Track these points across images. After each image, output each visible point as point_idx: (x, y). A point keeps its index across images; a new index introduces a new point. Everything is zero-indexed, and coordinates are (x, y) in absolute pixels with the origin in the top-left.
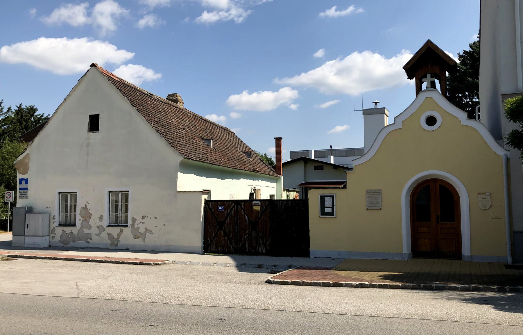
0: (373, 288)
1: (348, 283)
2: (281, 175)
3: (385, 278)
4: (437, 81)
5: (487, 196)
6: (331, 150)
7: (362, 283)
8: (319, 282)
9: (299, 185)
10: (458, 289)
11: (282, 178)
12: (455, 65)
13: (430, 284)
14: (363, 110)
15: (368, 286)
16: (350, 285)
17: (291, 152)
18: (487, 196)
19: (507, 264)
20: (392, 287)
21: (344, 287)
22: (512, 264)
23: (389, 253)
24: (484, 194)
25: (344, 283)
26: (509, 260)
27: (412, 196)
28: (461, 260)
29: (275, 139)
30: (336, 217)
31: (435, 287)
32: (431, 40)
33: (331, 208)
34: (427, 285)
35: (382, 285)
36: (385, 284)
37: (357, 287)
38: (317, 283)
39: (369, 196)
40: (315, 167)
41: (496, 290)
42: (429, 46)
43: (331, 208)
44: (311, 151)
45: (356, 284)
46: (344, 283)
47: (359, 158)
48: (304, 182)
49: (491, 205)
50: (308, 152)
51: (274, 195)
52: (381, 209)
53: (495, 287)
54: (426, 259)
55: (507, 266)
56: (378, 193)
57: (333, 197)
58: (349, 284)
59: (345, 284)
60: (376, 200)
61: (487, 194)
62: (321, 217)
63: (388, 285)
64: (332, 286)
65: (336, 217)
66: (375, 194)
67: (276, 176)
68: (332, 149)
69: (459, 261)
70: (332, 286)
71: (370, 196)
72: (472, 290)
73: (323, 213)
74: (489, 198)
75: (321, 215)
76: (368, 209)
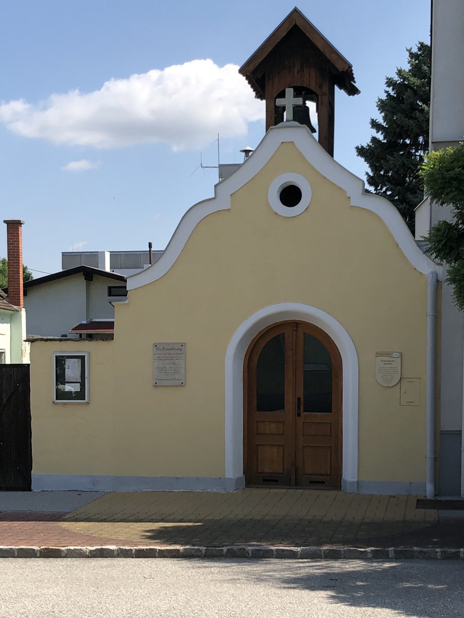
0: (125, 557)
1: (72, 548)
2: (22, 306)
3: (158, 535)
4: (311, 106)
5: (394, 359)
6: (150, 253)
7: (102, 549)
8: (11, 549)
9: (73, 329)
10: (297, 555)
11: (23, 313)
12: (347, 71)
13: (241, 547)
14: (221, 166)
15: (116, 553)
16: (77, 553)
17: (64, 254)
18: (394, 359)
19: (425, 498)
20: (163, 555)
21: (64, 557)
22: (433, 499)
23: (198, 479)
24: (388, 354)
25: (64, 548)
26: (429, 491)
27: (248, 357)
28: (341, 489)
29: (6, 224)
30: (88, 403)
31: (250, 553)
32: (300, 8)
33: (79, 384)
34: (234, 548)
35: (143, 550)
36: (150, 549)
37: (92, 557)
38: (6, 550)
39: (159, 356)
40: (110, 288)
41: (370, 555)
42: (295, 24)
43: (79, 384)
44: (103, 253)
45: (91, 551)
46: (64, 548)
47: (139, 274)
48: (85, 322)
49: (401, 378)
50: (96, 256)
51: (3, 351)
52: (183, 384)
53: (369, 549)
54: (271, 488)
55: (422, 503)
56: (179, 349)
57: (82, 358)
58: (75, 550)
59: (66, 552)
60: (172, 366)
61: (395, 355)
62: (57, 404)
63: (156, 549)
64: (38, 555)
65: (88, 403)
66: (172, 352)
67: (10, 310)
68: (152, 249)
69: (333, 493)
70: (38, 555)
71: (161, 355)
72: (323, 556)
73: (61, 395)
74: (397, 363)
75: (57, 399)
76: (156, 386)
